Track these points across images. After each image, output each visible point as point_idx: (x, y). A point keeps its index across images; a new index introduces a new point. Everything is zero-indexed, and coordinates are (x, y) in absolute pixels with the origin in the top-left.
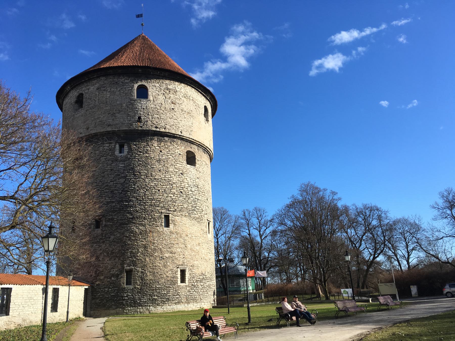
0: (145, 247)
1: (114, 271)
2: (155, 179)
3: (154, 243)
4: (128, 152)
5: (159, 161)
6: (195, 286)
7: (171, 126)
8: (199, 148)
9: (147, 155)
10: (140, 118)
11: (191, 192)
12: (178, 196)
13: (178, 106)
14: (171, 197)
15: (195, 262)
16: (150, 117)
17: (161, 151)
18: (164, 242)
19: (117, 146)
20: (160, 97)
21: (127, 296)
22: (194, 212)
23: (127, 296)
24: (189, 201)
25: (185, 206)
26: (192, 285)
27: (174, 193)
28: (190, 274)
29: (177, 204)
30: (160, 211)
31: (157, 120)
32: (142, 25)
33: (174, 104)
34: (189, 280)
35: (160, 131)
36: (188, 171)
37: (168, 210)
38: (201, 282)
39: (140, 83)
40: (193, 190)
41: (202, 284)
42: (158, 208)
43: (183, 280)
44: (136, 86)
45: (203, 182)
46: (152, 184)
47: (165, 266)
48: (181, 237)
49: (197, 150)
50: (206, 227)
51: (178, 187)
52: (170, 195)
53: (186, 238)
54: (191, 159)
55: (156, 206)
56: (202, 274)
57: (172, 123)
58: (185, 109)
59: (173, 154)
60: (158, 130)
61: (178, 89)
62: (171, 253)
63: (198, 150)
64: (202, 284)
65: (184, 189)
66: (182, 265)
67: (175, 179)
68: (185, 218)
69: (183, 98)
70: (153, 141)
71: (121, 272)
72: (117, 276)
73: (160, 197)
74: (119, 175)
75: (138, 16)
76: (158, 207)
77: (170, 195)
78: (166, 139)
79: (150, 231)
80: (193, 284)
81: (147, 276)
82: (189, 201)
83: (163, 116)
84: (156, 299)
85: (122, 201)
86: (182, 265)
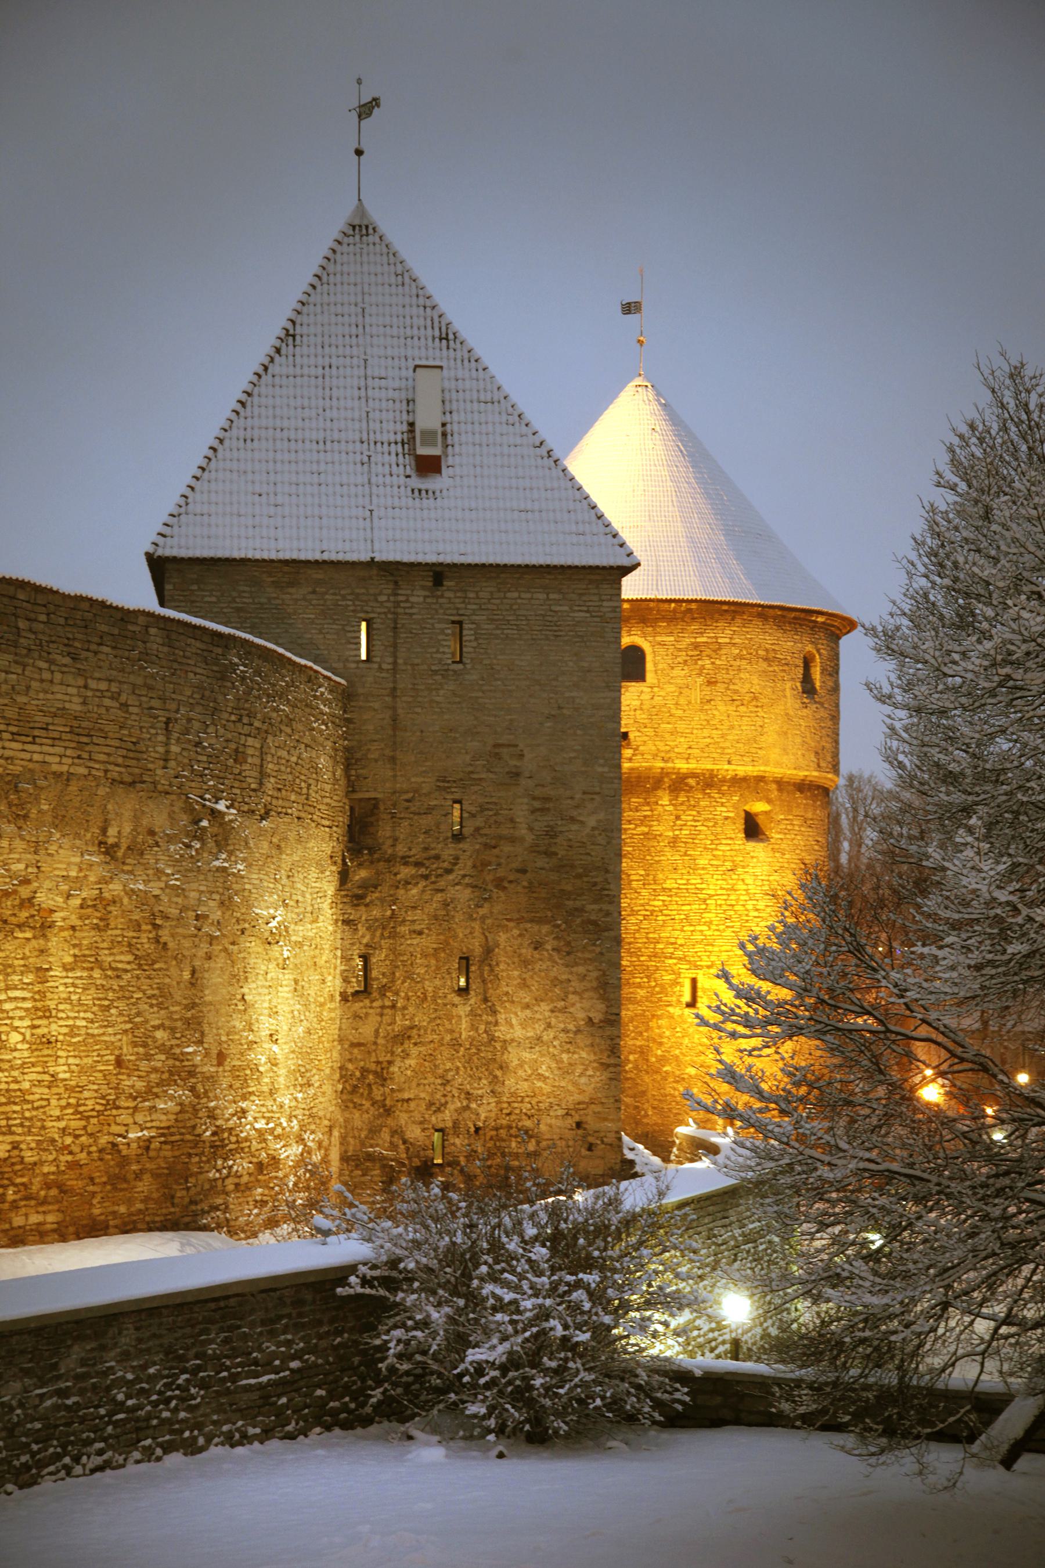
2: (664, 889)
3: (661, 1044)
5: (674, 842)
7: (702, 750)
11: (756, 914)
12: (722, 927)
13: (721, 687)
17: (678, 818)
18: (686, 1041)
20: (677, 672)
29: (716, 949)
30: (676, 968)
31: (667, 735)
40: (761, 905)
42: (671, 961)
46: (656, 903)
57: (708, 740)
59: (708, 820)
60: (670, 765)
69: (738, 663)
70: (660, 793)
75: (629, 308)
77: (699, 928)
81: (646, 1116)
83: (681, 726)
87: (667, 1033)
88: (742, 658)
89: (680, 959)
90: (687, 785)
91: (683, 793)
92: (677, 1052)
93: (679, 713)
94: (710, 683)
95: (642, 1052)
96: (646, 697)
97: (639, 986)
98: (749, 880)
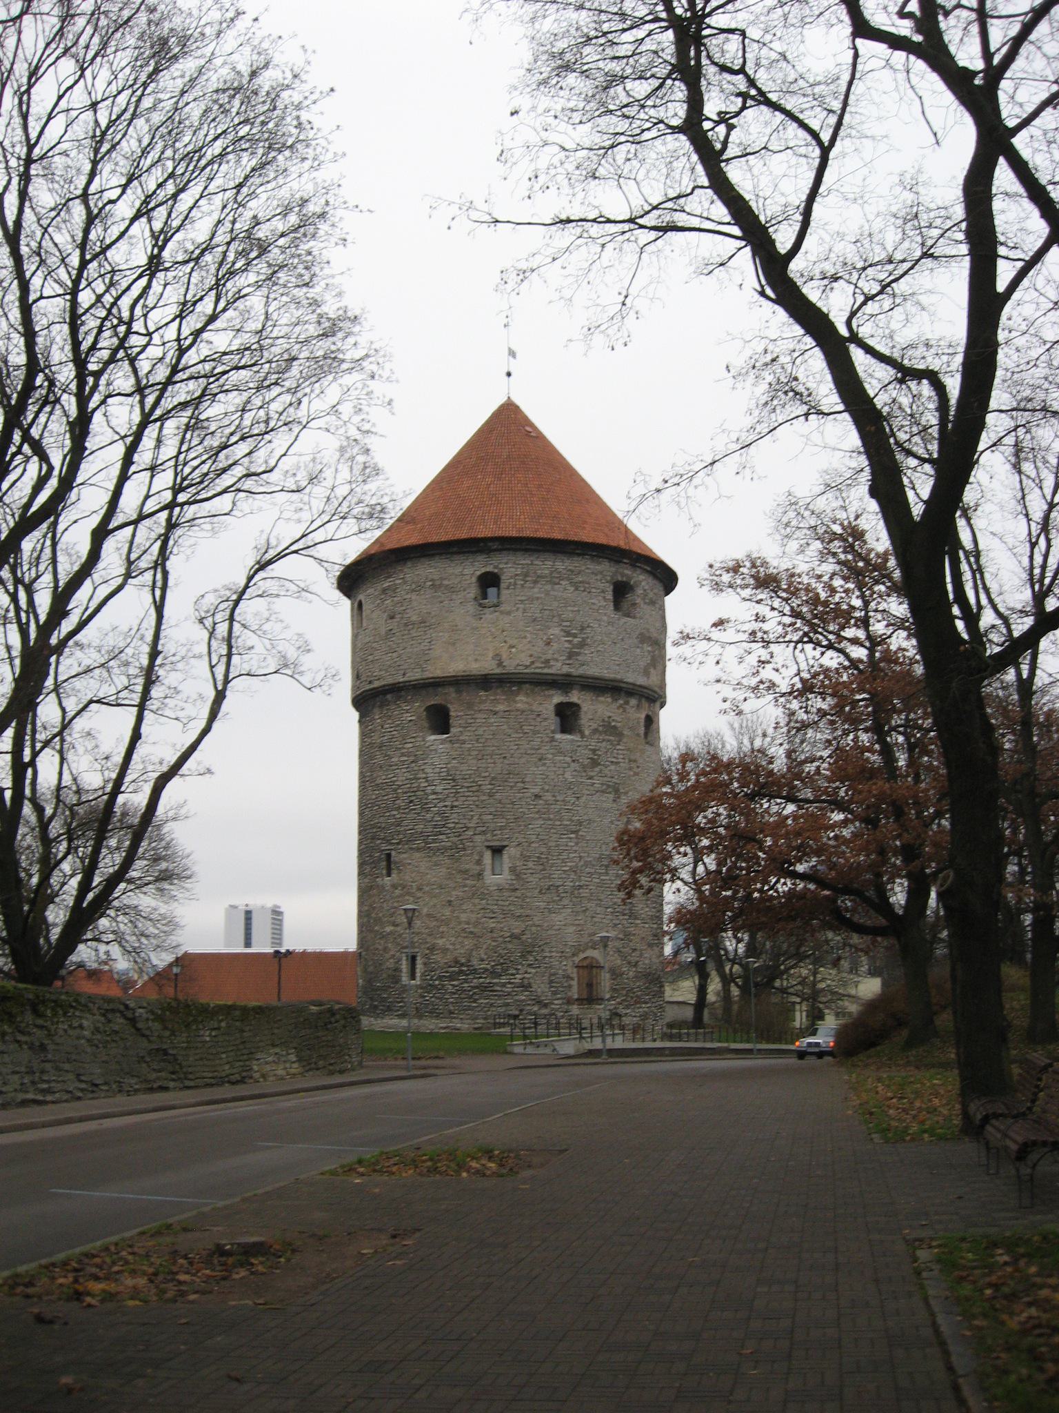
6: (435, 987)
15: (440, 942)
25: (420, 827)
28: (425, 964)
32: (509, 374)
34: (423, 975)
38: (451, 978)
40: (439, 789)
43: (413, 977)
47: (385, 949)
48: (408, 894)
49: (454, 695)
50: (479, 862)
56: (457, 962)
58: (414, 618)
60: (372, 686)
63: (459, 692)
68: (417, 855)
78: (389, 697)
82: (428, 816)
88: (413, 591)
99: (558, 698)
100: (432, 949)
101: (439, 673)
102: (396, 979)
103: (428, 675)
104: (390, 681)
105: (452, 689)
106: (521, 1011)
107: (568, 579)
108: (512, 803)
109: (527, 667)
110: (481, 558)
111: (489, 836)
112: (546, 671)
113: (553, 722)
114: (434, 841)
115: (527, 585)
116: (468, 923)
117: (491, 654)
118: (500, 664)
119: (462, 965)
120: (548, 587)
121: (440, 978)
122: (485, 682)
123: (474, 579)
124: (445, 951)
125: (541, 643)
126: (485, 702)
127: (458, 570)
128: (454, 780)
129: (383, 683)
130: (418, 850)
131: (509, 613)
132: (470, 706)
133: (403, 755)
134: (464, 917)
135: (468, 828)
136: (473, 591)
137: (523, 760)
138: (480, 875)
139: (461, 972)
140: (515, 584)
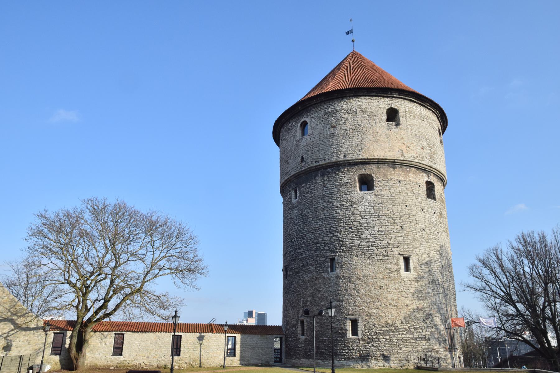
0: (313, 296)
1: (294, 322)
3: (320, 291)
4: (299, 196)
6: (373, 340)
8: (380, 166)
9: (312, 195)
10: (302, 157)
14: (337, 236)
15: (374, 311)
16: (310, 153)
17: (324, 186)
18: (331, 289)
19: (293, 193)
21: (301, 347)
22: (372, 248)
23: (301, 347)
24: (363, 236)
26: (369, 338)
27: (341, 231)
28: (365, 325)
32: (353, 41)
33: (334, 127)
35: (320, 165)
36: (360, 199)
37: (334, 252)
39: (302, 121)
40: (369, 220)
41: (388, 337)
42: (323, 252)
44: (299, 124)
45: (391, 206)
46: (317, 226)
48: (350, 282)
49: (375, 169)
50: (397, 264)
51: (346, 223)
52: (335, 234)
53: (358, 282)
54: (367, 183)
55: (321, 250)
56: (387, 324)
60: (318, 164)
61: (338, 108)
62: (338, 301)
63: (378, 168)
64: (388, 337)
65: (354, 223)
66: (352, 315)
67: (341, 215)
70: (317, 178)
71: (297, 322)
72: (295, 326)
73: (325, 239)
74: (294, 222)
76: (323, 250)
77: (335, 234)
78: (330, 170)
79: (317, 278)
80: (370, 337)
82: (363, 236)
83: (322, 147)
84: (323, 353)
85: (296, 249)
86: (352, 315)
87: (322, 286)
89: (327, 250)
90: (327, 172)
91: (326, 176)
92: (327, 295)
93: (321, 142)
94: (332, 127)
95: (313, 296)
96: (309, 139)
97: (312, 265)
98: (361, 209)
99: (426, 179)
100: (370, 315)
101: (367, 156)
102: (344, 335)
103: (360, 157)
104: (334, 159)
105: (374, 167)
106: (426, 355)
107: (427, 120)
108: (412, 231)
109: (415, 158)
110: (388, 100)
111: (401, 249)
112: (423, 162)
113: (423, 190)
114: (368, 250)
115: (411, 117)
116: (393, 300)
117: (397, 149)
118: (402, 155)
119: (391, 326)
120: (420, 121)
121: (376, 334)
122: (393, 163)
123: (385, 111)
124: (378, 317)
125: (420, 148)
126: (394, 174)
127: (376, 104)
128: (378, 216)
129: (327, 161)
130: (357, 255)
131: (404, 130)
132: (385, 176)
133: (342, 201)
134: (389, 296)
135: (389, 244)
136: (385, 117)
137: (415, 208)
138: (398, 271)
139: (390, 330)
140: (406, 116)
